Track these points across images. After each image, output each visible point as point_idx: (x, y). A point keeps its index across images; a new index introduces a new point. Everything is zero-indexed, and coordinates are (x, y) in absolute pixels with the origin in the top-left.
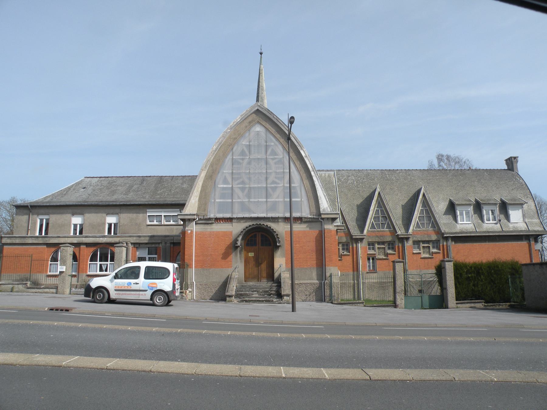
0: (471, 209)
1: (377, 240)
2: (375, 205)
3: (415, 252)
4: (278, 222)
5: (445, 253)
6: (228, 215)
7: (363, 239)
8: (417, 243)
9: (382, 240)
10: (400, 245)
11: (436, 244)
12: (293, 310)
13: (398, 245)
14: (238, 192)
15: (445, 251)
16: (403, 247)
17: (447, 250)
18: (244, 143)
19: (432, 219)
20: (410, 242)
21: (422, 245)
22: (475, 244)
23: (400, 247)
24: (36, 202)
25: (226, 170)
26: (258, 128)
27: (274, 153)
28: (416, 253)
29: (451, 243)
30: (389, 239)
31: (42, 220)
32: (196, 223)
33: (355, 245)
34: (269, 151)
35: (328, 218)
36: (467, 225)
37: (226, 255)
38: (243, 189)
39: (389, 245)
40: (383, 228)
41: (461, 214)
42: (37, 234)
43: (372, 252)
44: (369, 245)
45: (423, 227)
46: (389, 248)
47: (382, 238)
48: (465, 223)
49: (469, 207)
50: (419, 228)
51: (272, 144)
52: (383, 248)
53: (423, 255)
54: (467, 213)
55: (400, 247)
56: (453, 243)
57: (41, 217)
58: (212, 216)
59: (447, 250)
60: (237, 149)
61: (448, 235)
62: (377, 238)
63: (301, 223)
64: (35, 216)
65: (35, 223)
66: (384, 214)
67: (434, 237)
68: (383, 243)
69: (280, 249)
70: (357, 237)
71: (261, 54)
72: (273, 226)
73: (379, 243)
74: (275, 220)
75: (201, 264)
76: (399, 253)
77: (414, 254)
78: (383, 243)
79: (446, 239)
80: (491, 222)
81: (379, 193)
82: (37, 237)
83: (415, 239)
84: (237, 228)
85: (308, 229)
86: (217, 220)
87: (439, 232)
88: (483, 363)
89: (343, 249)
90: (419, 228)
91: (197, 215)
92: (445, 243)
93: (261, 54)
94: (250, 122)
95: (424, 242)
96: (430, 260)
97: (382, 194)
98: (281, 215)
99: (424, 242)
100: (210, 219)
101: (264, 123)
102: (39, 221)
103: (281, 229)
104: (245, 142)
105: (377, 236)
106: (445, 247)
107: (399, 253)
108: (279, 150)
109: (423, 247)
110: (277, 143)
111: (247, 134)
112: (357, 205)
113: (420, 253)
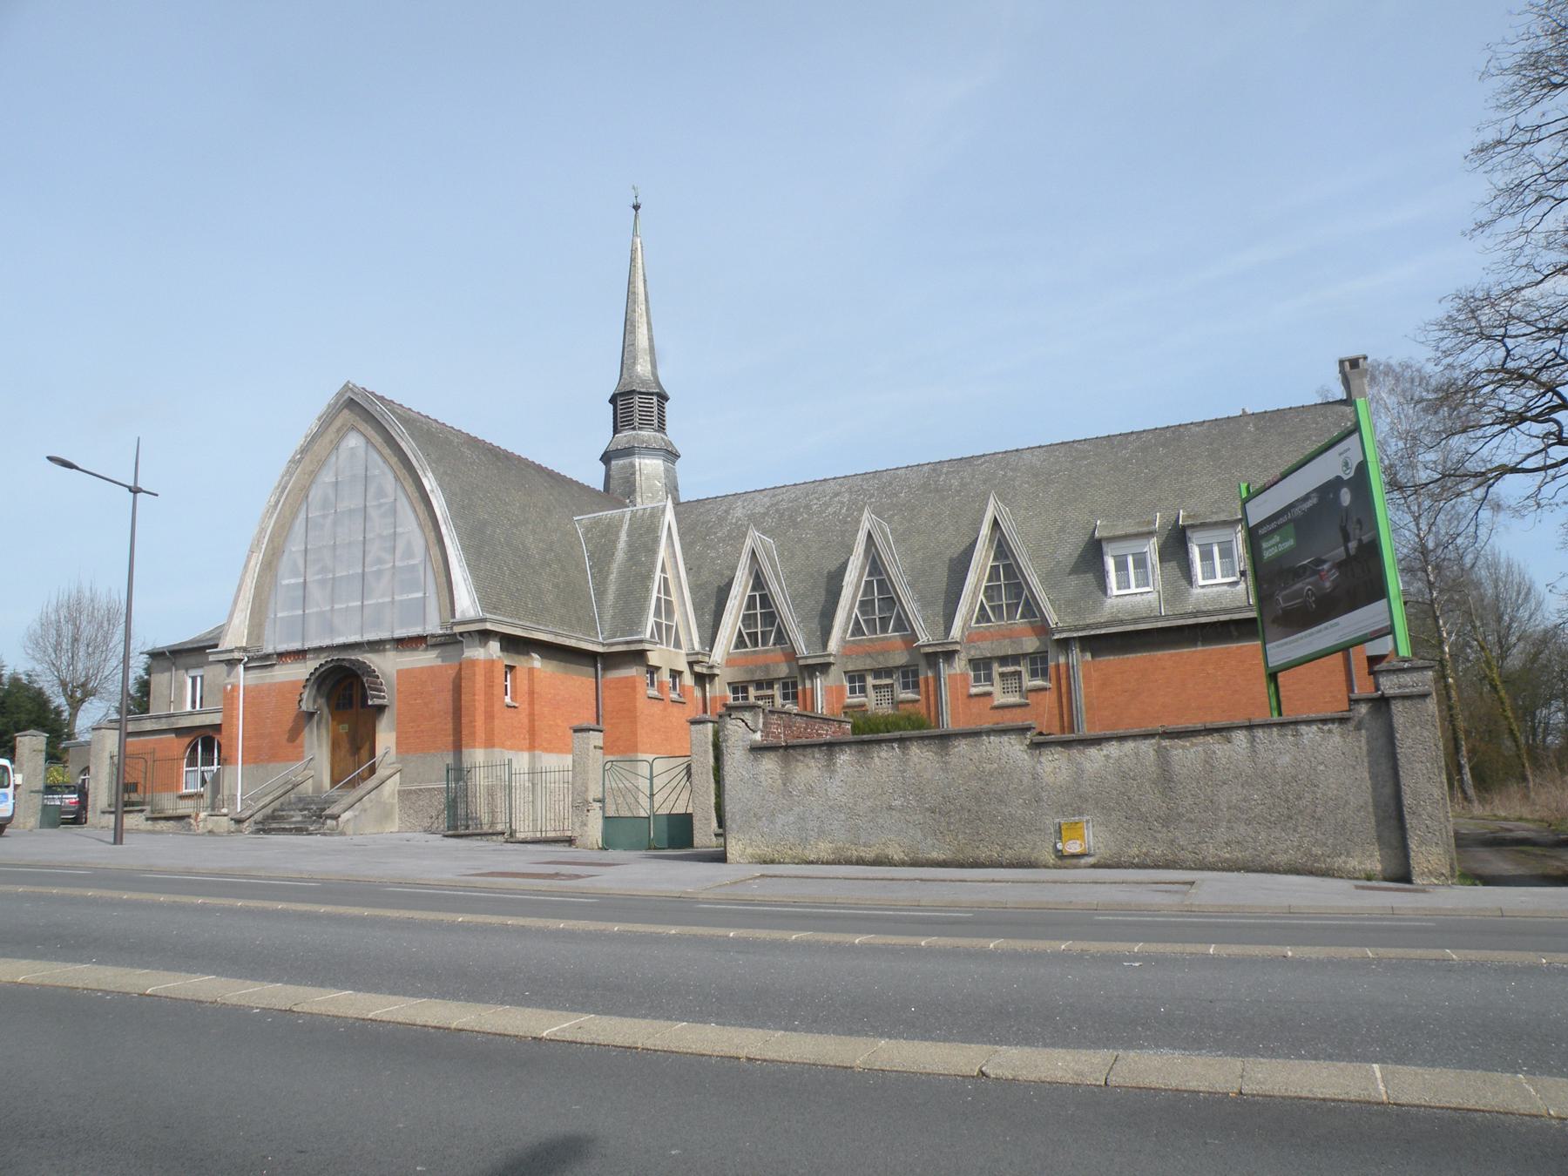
0: (1151, 548)
1: (869, 664)
2: (863, 568)
3: (974, 691)
4: (384, 650)
5: (1064, 689)
6: (296, 646)
7: (829, 665)
8: (981, 665)
9: (882, 663)
10: (930, 674)
11: (1038, 663)
12: (118, 839)
13: (926, 674)
14: (315, 592)
15: (1063, 682)
16: (937, 678)
17: (1068, 678)
18: (327, 480)
19: (1026, 591)
20: (960, 665)
21: (997, 669)
22: (1159, 654)
23: (931, 681)
24: (191, 642)
25: (295, 547)
26: (353, 441)
27: (381, 493)
28: (977, 695)
29: (1078, 658)
30: (900, 658)
31: (194, 679)
32: (246, 669)
33: (808, 685)
34: (372, 490)
35: (469, 633)
36: (1139, 598)
37: (294, 734)
38: (322, 582)
39: (905, 675)
40: (884, 629)
41: (1206, 556)
42: (188, 708)
43: (857, 699)
44: (851, 680)
45: (1000, 617)
46: (906, 686)
47: (881, 658)
48: (1133, 592)
49: (1144, 541)
50: (989, 620)
51: (377, 472)
52: (887, 686)
53: (1000, 699)
54: (1141, 562)
55: (931, 681)
56: (1088, 656)
57: (193, 673)
58: (269, 649)
59: (1068, 678)
60: (316, 494)
61: (1064, 635)
62: (869, 661)
63: (426, 650)
64: (182, 672)
65: (182, 687)
66: (1008, 580)
67: (1031, 644)
68: (888, 672)
69: (387, 713)
70: (810, 662)
71: (636, 207)
72: (373, 660)
73: (877, 673)
74: (376, 646)
75: (253, 756)
76: (928, 698)
77: (970, 696)
78: (888, 672)
79: (1064, 644)
80: (1219, 580)
81: (870, 535)
82: (191, 714)
83: (975, 654)
84: (300, 671)
85: (439, 662)
86: (282, 655)
87: (1043, 629)
88: (1400, 1039)
89: (785, 697)
90: (989, 620)
91: (245, 650)
92: (1062, 660)
93: (636, 207)
94: (338, 430)
95: (1004, 660)
96: (1019, 711)
97: (877, 538)
98: (385, 635)
99: (1004, 660)
100: (267, 657)
101: (363, 427)
102: (189, 682)
103: (387, 665)
104: (327, 477)
105: (869, 655)
106: (1063, 670)
107: (928, 698)
108: (389, 482)
109: (1002, 675)
110: (387, 470)
111: (333, 459)
112: (951, 560)
113: (989, 694)
